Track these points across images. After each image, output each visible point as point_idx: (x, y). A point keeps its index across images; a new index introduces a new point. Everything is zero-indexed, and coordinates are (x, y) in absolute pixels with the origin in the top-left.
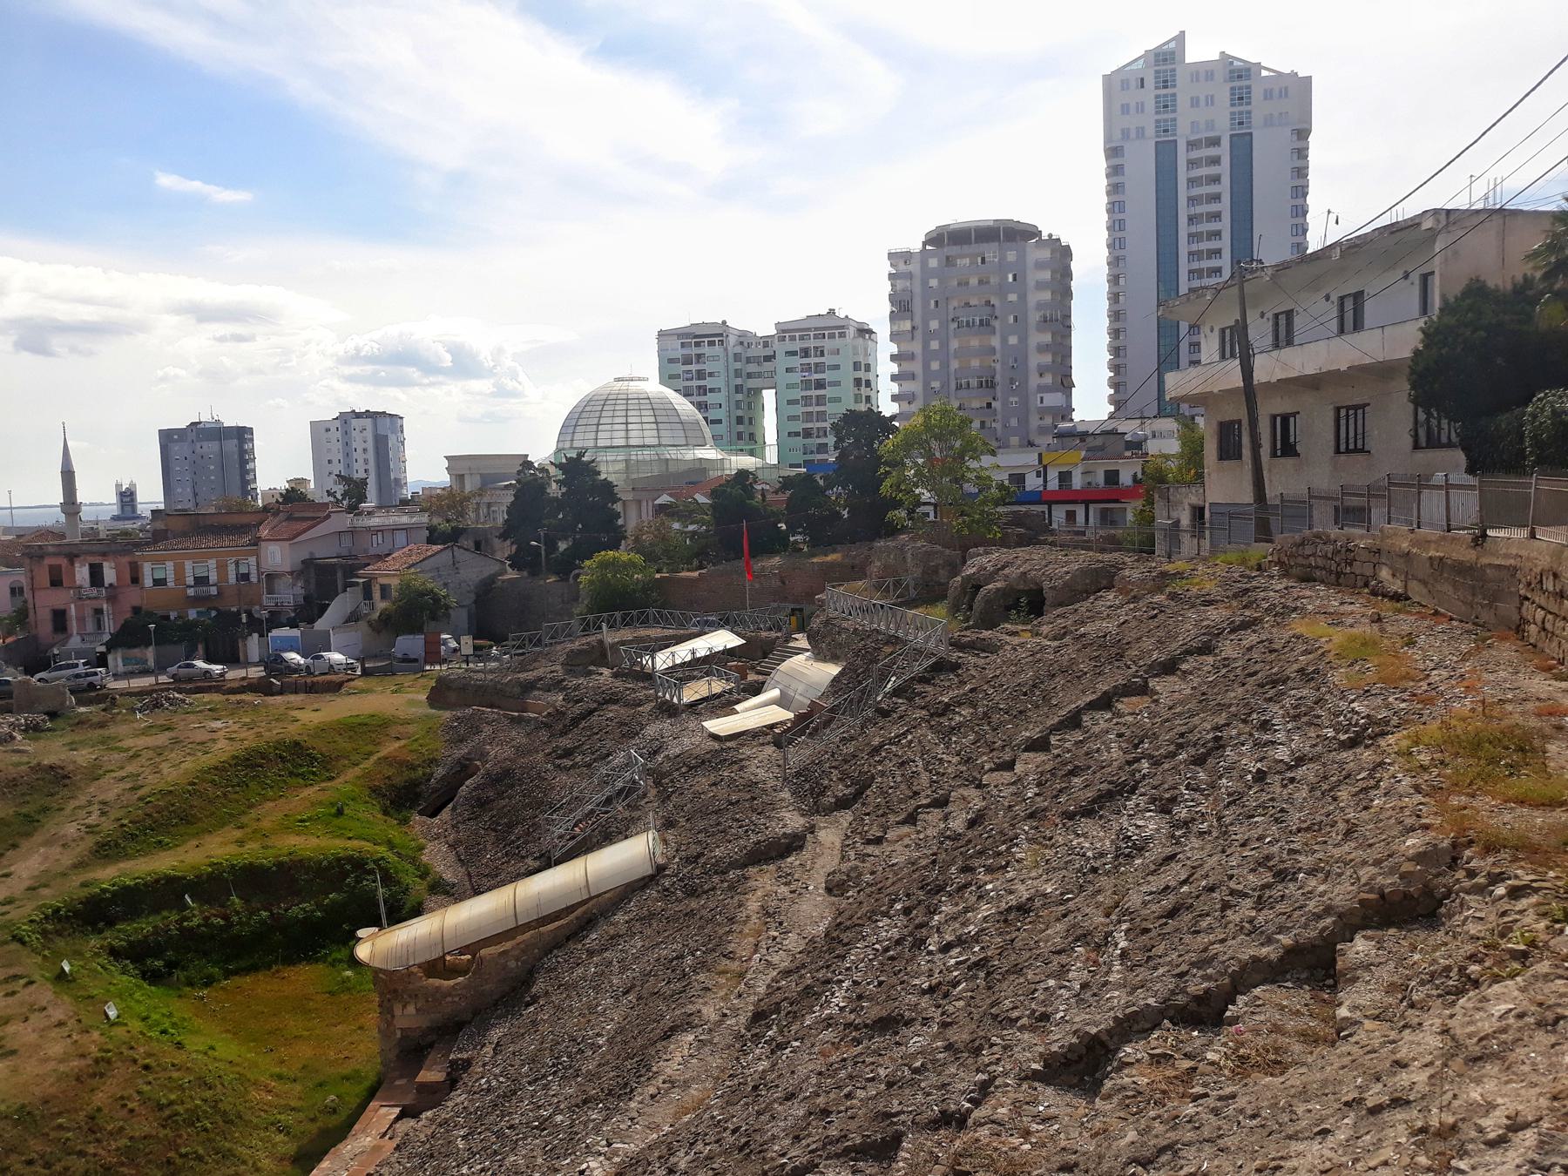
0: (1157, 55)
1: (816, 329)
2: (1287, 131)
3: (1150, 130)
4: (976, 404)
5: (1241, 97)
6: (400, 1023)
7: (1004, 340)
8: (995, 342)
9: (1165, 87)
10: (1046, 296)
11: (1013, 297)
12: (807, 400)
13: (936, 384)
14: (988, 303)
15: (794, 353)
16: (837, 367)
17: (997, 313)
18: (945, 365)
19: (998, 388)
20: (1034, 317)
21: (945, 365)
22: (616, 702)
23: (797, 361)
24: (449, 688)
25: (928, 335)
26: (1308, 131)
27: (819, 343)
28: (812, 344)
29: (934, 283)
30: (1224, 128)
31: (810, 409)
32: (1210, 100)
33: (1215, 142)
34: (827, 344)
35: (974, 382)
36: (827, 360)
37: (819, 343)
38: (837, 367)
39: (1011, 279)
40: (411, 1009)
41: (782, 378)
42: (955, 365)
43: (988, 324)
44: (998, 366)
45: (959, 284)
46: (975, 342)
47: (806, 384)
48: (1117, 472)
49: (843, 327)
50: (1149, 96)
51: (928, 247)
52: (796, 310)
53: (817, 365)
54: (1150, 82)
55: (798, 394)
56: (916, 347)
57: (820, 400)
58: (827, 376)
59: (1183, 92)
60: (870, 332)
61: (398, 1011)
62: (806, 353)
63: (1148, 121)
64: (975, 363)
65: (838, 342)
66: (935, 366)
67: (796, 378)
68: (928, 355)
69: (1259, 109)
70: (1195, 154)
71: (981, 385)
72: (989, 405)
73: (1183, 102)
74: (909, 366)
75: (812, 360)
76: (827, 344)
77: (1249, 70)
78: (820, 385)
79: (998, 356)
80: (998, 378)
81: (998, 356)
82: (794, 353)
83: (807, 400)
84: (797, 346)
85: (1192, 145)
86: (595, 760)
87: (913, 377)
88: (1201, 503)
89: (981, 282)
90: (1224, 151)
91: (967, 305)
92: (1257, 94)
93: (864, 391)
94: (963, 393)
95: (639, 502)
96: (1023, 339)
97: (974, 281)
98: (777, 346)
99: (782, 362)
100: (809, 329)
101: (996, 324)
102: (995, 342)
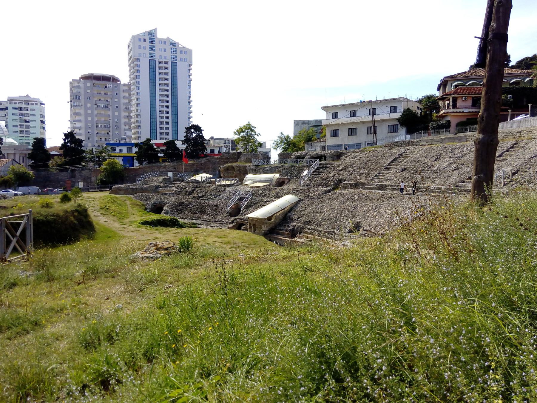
0: (149, 33)
1: (25, 101)
2: (186, 64)
3: (148, 55)
4: (103, 132)
5: (174, 51)
6: (264, 229)
7: (113, 113)
8: (110, 113)
9: (152, 43)
10: (126, 101)
11: (116, 100)
12: (21, 126)
13: (90, 125)
14: (107, 101)
15: (16, 109)
16: (34, 115)
17: (111, 104)
18: (92, 119)
19: (111, 128)
20: (123, 107)
21: (92, 119)
22: (199, 187)
23: (17, 112)
24: (120, 190)
25: (87, 108)
26: (192, 65)
27: (27, 106)
28: (24, 106)
29: (89, 91)
30: (169, 60)
31: (23, 129)
32: (160, 50)
33: (166, 63)
34: (30, 107)
35: (103, 125)
36: (29, 112)
37: (27, 106)
38: (34, 115)
39: (115, 94)
40: (266, 227)
41: (10, 117)
42: (96, 119)
43: (108, 107)
44: (111, 121)
45: (97, 93)
46: (103, 112)
47: (21, 120)
48: (214, 150)
49: (36, 101)
50: (147, 44)
51: (81, 80)
52: (15, 94)
53: (25, 114)
54: (147, 40)
55: (18, 124)
56: (82, 111)
57: (27, 127)
58: (30, 118)
59: (157, 45)
60: (44, 104)
61: (263, 226)
62: (21, 109)
63: (147, 52)
64: (103, 119)
65: (34, 107)
66: (89, 118)
67: (17, 117)
68: (86, 115)
69: (179, 56)
70: (161, 65)
71: (105, 126)
72: (108, 133)
73: (157, 49)
74: (78, 118)
75: (24, 112)
76: (30, 107)
77: (175, 44)
78: (27, 121)
79: (111, 118)
80: (111, 125)
81: (111, 118)
82: (16, 109)
83: (21, 126)
84: (17, 106)
85: (160, 62)
86: (217, 196)
87: (80, 121)
88: (325, 145)
89: (105, 94)
90: (169, 66)
91: (100, 100)
92: (178, 51)
93: (44, 125)
94: (100, 129)
95: (15, 154)
96: (119, 114)
97: (102, 93)
98: (10, 107)
99: (10, 111)
100: (22, 101)
101: (110, 107)
102: (110, 113)
